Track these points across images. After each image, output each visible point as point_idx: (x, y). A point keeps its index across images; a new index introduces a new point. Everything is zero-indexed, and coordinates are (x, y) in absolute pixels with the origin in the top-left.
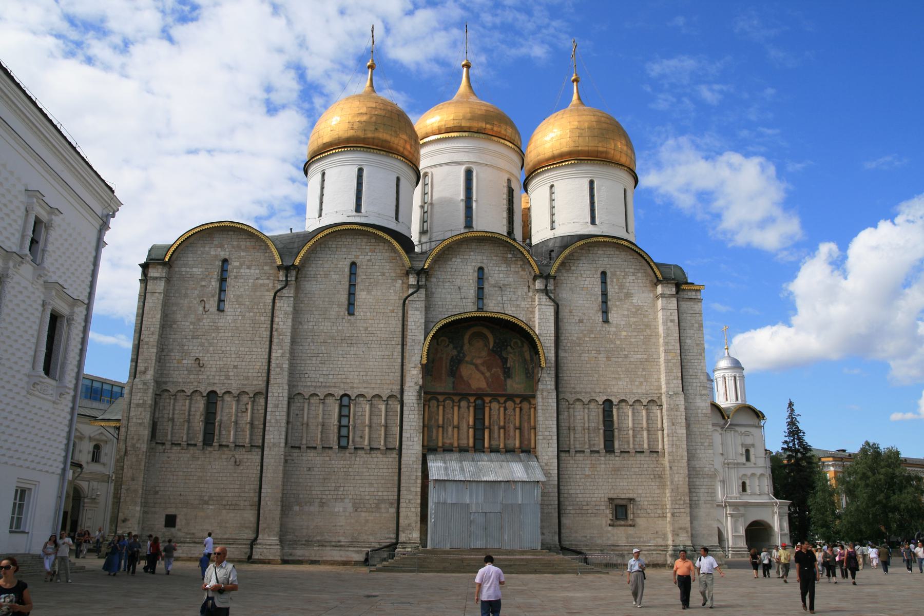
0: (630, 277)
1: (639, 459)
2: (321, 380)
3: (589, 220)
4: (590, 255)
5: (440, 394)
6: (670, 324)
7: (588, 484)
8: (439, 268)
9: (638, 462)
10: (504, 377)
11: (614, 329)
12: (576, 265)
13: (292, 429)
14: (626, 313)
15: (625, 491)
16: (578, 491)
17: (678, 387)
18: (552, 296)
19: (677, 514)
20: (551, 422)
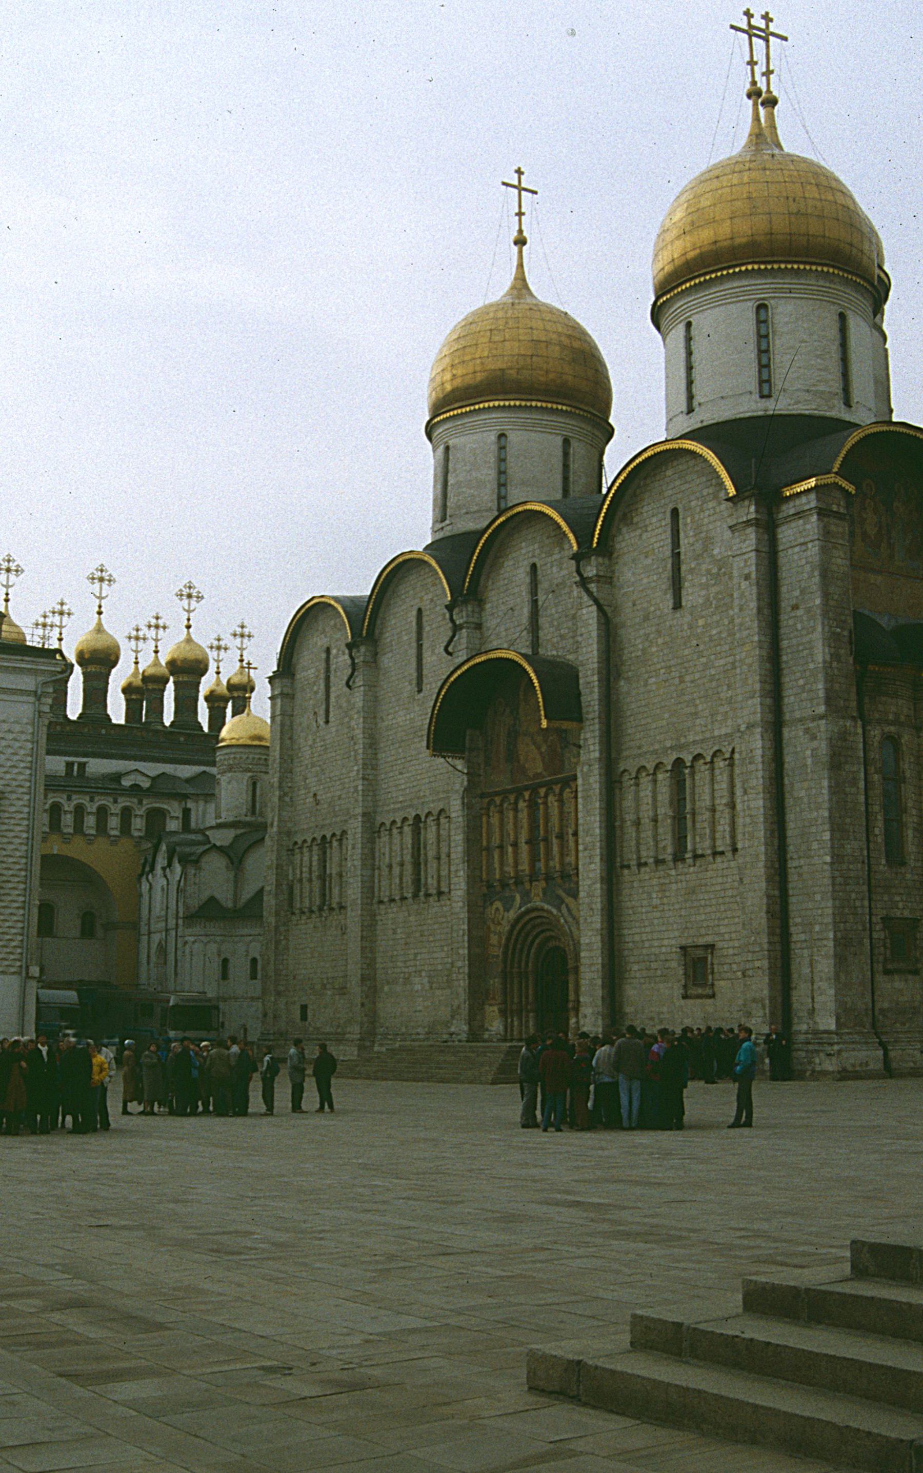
0: (711, 505)
1: (721, 866)
2: (401, 799)
3: (684, 408)
4: (657, 484)
5: (497, 794)
6: (745, 584)
7: (656, 921)
8: (493, 583)
9: (720, 873)
10: (561, 748)
11: (688, 618)
12: (640, 510)
13: (380, 875)
14: (704, 580)
15: (703, 931)
16: (644, 937)
17: (755, 713)
18: (593, 587)
19: (750, 973)
20: (593, 818)
